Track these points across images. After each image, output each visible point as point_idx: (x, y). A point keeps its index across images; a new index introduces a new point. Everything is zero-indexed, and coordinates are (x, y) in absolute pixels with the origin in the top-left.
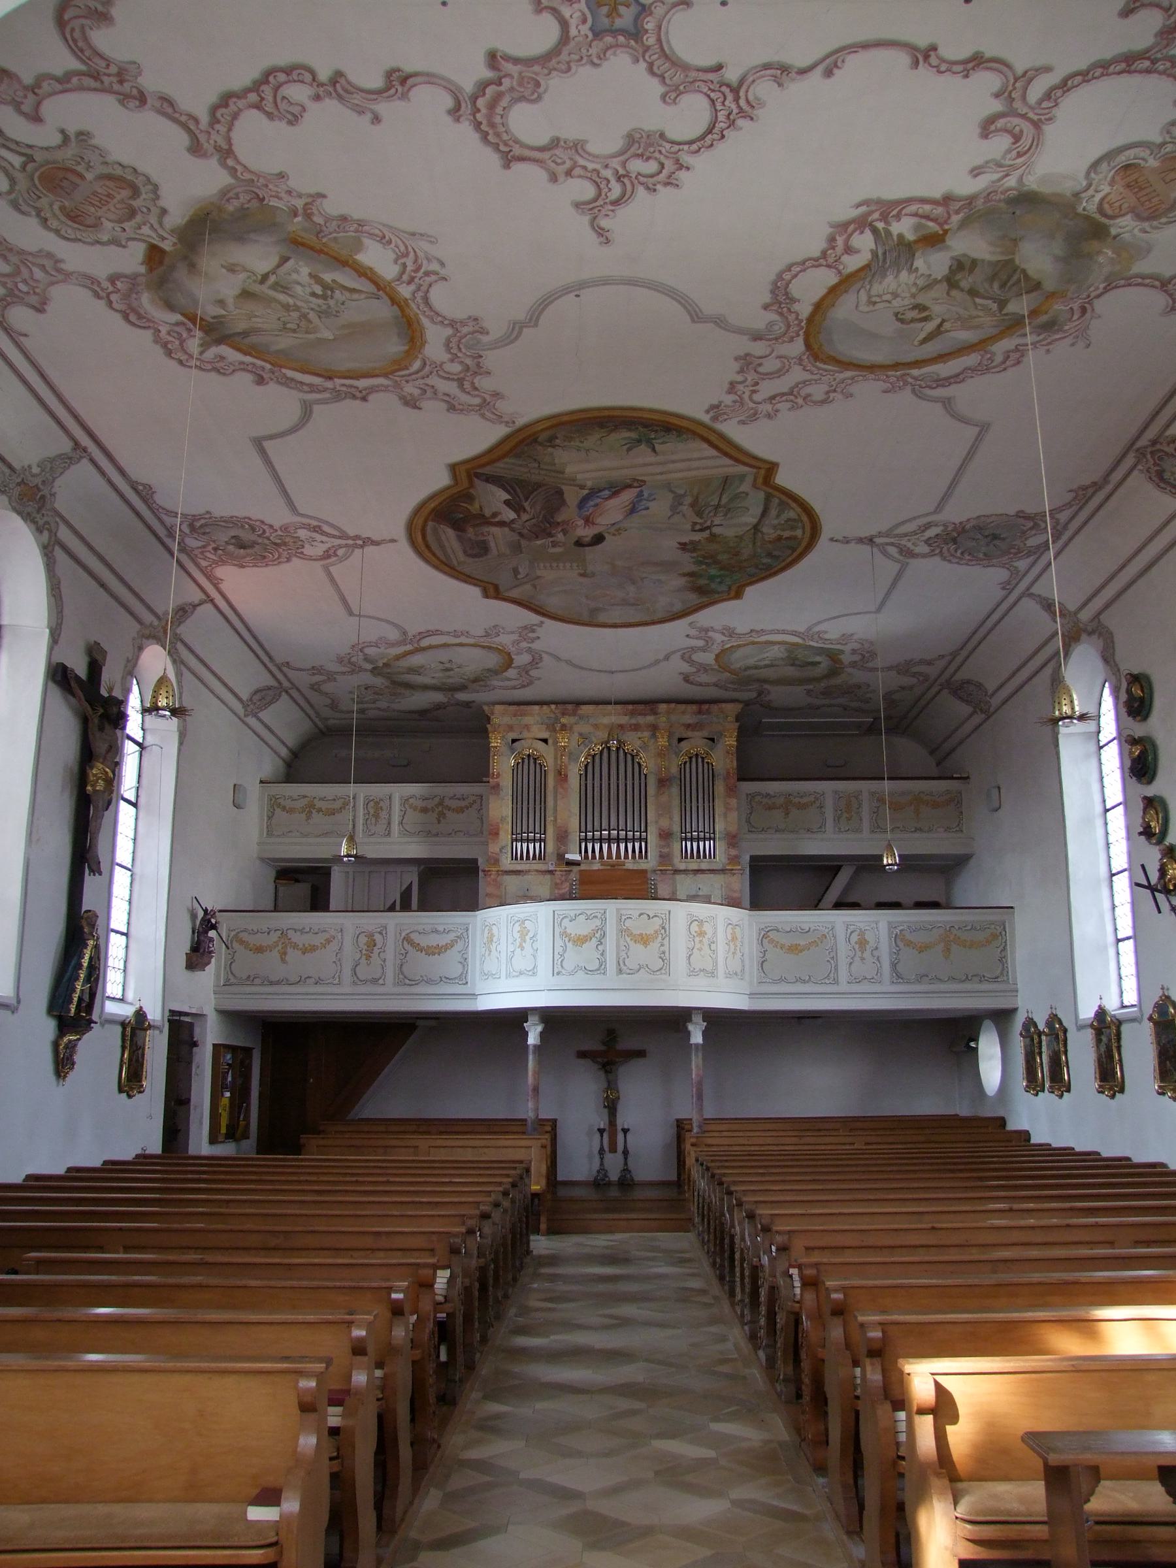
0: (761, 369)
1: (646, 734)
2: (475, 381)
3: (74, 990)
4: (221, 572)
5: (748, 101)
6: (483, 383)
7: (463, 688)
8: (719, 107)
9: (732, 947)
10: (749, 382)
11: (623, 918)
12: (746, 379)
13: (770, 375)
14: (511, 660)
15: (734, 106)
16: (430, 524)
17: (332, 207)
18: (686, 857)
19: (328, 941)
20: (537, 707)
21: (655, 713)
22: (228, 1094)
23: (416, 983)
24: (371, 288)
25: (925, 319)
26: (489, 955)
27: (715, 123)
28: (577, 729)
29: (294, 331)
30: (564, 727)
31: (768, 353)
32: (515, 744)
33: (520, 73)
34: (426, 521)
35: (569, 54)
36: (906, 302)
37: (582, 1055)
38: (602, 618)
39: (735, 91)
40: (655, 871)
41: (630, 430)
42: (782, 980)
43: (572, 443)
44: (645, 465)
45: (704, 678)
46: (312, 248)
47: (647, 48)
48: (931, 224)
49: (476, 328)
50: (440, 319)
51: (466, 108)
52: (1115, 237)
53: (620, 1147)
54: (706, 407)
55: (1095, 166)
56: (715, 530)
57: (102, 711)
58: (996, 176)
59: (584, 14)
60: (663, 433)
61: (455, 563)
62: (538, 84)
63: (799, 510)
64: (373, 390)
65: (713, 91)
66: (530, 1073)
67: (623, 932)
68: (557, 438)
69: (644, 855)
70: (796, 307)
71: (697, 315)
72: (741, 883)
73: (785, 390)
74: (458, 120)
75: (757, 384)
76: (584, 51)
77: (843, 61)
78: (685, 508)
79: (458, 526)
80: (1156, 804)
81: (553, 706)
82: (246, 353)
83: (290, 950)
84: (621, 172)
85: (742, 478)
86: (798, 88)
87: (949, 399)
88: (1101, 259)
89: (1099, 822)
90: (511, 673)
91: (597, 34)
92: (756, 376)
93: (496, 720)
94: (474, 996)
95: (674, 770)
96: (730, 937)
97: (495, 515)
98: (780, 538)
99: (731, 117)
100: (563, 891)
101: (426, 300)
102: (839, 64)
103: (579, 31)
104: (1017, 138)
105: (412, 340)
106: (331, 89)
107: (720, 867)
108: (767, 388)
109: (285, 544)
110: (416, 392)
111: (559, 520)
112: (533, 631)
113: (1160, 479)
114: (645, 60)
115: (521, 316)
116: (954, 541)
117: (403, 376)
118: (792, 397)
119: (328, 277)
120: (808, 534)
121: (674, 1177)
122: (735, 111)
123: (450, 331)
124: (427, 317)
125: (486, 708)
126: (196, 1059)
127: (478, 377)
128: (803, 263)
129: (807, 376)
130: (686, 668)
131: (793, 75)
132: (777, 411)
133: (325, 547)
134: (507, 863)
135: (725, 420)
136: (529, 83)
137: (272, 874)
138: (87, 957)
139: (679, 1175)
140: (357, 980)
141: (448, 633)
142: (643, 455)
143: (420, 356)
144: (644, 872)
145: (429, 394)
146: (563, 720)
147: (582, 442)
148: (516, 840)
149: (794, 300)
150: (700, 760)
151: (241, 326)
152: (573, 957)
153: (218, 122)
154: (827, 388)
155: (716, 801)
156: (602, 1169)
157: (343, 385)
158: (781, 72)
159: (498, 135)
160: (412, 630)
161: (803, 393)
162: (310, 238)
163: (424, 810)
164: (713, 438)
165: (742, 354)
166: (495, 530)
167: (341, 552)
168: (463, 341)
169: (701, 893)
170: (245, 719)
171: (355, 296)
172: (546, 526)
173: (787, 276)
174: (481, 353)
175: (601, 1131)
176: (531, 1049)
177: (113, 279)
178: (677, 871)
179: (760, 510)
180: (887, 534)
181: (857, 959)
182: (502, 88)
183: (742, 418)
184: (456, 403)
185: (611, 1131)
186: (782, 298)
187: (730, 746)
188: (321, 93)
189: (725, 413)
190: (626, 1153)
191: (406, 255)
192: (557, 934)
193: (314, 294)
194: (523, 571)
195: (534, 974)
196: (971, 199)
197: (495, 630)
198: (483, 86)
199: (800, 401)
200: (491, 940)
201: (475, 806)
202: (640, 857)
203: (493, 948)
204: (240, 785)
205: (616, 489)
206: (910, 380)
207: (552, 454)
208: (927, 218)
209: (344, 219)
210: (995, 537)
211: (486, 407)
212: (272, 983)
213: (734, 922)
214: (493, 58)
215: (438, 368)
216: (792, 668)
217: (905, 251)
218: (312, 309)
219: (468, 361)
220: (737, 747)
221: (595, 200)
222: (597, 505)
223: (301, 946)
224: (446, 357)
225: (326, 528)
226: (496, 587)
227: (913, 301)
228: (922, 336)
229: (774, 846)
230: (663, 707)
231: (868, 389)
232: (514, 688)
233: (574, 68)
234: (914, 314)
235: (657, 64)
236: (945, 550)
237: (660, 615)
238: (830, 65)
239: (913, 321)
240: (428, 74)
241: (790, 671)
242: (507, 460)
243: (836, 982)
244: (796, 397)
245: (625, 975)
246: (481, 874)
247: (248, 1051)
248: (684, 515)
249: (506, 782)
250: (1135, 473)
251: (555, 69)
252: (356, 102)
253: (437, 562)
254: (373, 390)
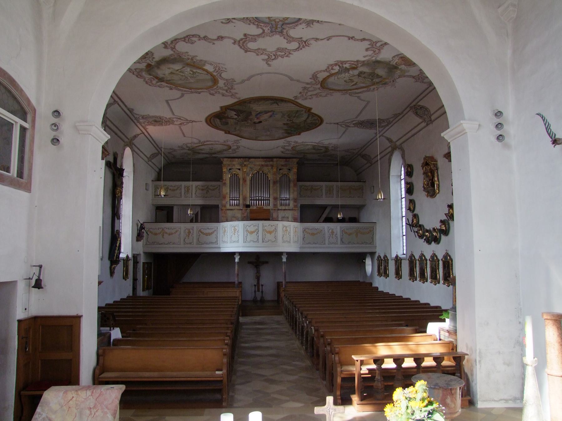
1: (270, 168)
3: (115, 253)
4: (147, 127)
5: (308, 43)
6: (233, 91)
7: (215, 153)
9: (295, 234)
11: (264, 226)
13: (310, 91)
14: (231, 148)
17: (198, 58)
18: (281, 205)
19: (176, 232)
20: (237, 159)
21: (272, 161)
22: (146, 277)
23: (202, 244)
24: (207, 73)
25: (352, 82)
26: (225, 236)
28: (249, 166)
29: (183, 80)
30: (245, 165)
32: (231, 170)
34: (211, 118)
36: (348, 79)
37: (249, 263)
38: (259, 139)
40: (272, 209)
41: (271, 101)
42: (309, 243)
45: (288, 152)
46: (192, 66)
48: (353, 65)
52: (400, 69)
53: (261, 290)
55: (394, 57)
56: (293, 121)
57: (119, 173)
58: (369, 58)
61: (218, 126)
63: (317, 117)
66: (236, 270)
67: (264, 230)
69: (269, 205)
70: (318, 79)
72: (297, 214)
78: (286, 116)
79: (220, 119)
80: (412, 202)
81: (242, 159)
82: (168, 84)
83: (165, 234)
84: (275, 54)
85: (302, 111)
86: (320, 42)
87: (359, 96)
88: (397, 72)
89: (400, 201)
90: (230, 150)
91: (271, 32)
92: (307, 91)
93: (224, 163)
94: (220, 248)
95: (278, 179)
96: (294, 231)
97: (231, 117)
98: (312, 123)
100: (245, 215)
101: (220, 75)
104: (374, 52)
107: (291, 208)
108: (309, 93)
109: (169, 121)
111: (250, 118)
112: (238, 141)
113: (416, 114)
116: (361, 124)
118: (317, 95)
119: (195, 71)
120: (320, 121)
121: (276, 299)
123: (225, 81)
125: (221, 159)
126: (138, 267)
128: (321, 71)
129: (320, 91)
130: (282, 150)
132: (313, 98)
133: (180, 122)
134: (228, 207)
137: (155, 208)
138: (118, 243)
139: (278, 299)
140: (185, 243)
141: (213, 141)
142: (275, 106)
144: (269, 209)
145: (218, 92)
146: (245, 163)
148: (231, 200)
149: (317, 78)
150: (286, 175)
151: (169, 79)
152: (249, 237)
153: (173, 43)
154: (326, 94)
155: (291, 188)
156: (255, 297)
158: (317, 39)
159: (244, 47)
160: (202, 140)
161: (320, 94)
162: (192, 64)
163: (202, 190)
164: (294, 103)
166: (232, 120)
167: (185, 123)
169: (285, 216)
170: (148, 163)
171: (201, 74)
172: (246, 119)
173: (316, 73)
175: (255, 285)
176: (236, 263)
177: (136, 69)
178: (278, 210)
179: (306, 117)
180: (342, 122)
181: (331, 238)
183: (303, 99)
185: (258, 285)
187: (295, 172)
190: (262, 292)
191: (217, 67)
192: (245, 231)
193: (190, 74)
194: (237, 128)
195: (238, 242)
196: (364, 61)
197: (227, 141)
198: (242, 39)
199: (319, 96)
200: (225, 231)
201: (218, 188)
202: (268, 205)
203: (226, 234)
204: (148, 184)
205: (266, 112)
208: (353, 64)
209: (201, 60)
210: (372, 123)
211: (233, 96)
212: (160, 244)
213: (296, 226)
214: (245, 35)
215: (221, 88)
216: (314, 150)
217: (347, 70)
218: (189, 76)
219: (230, 87)
220: (297, 172)
221: (268, 59)
222: (261, 115)
223: (168, 233)
224: (224, 86)
225: (182, 118)
228: (351, 85)
229: (307, 201)
230: (275, 160)
231: (338, 94)
232: (231, 154)
236: (358, 125)
237: (276, 138)
238: (329, 39)
239: (349, 82)
241: (314, 151)
243: (325, 244)
245: (265, 243)
246: (220, 209)
247: (151, 263)
249: (228, 182)
250: (410, 112)
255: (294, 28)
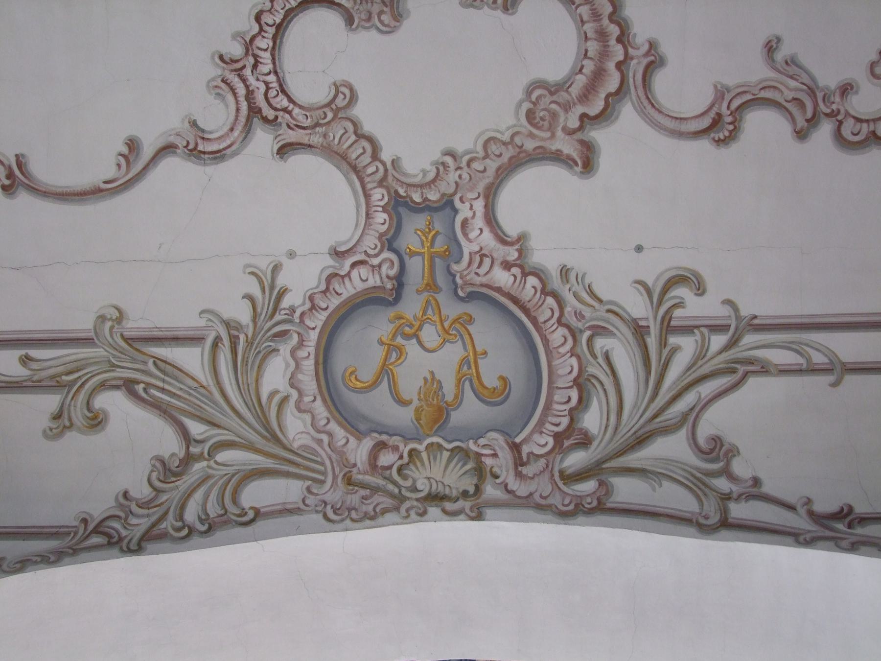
8: (272, 78)
15: (252, 80)
27: (274, 48)
33: (553, 136)
35: (485, 170)
39: (254, 111)
47: (381, 183)
51: (636, 68)
59: (465, 235)
62: (530, 116)
65: (285, 110)
74: (652, 45)
76: (465, 176)
77: (119, 165)
91: (447, 204)
99: (251, 60)
102: (123, 161)
103: (471, 208)
106: (822, 107)
114: (384, 164)
122: (248, 72)
131: (181, 143)
136: (542, 119)
182: (580, 109)
188: (837, 99)
198: (605, 116)
233: (479, 148)
235: (366, 159)
240: (680, 135)
251: (505, 144)
252: (793, 84)
255: (337, 254)
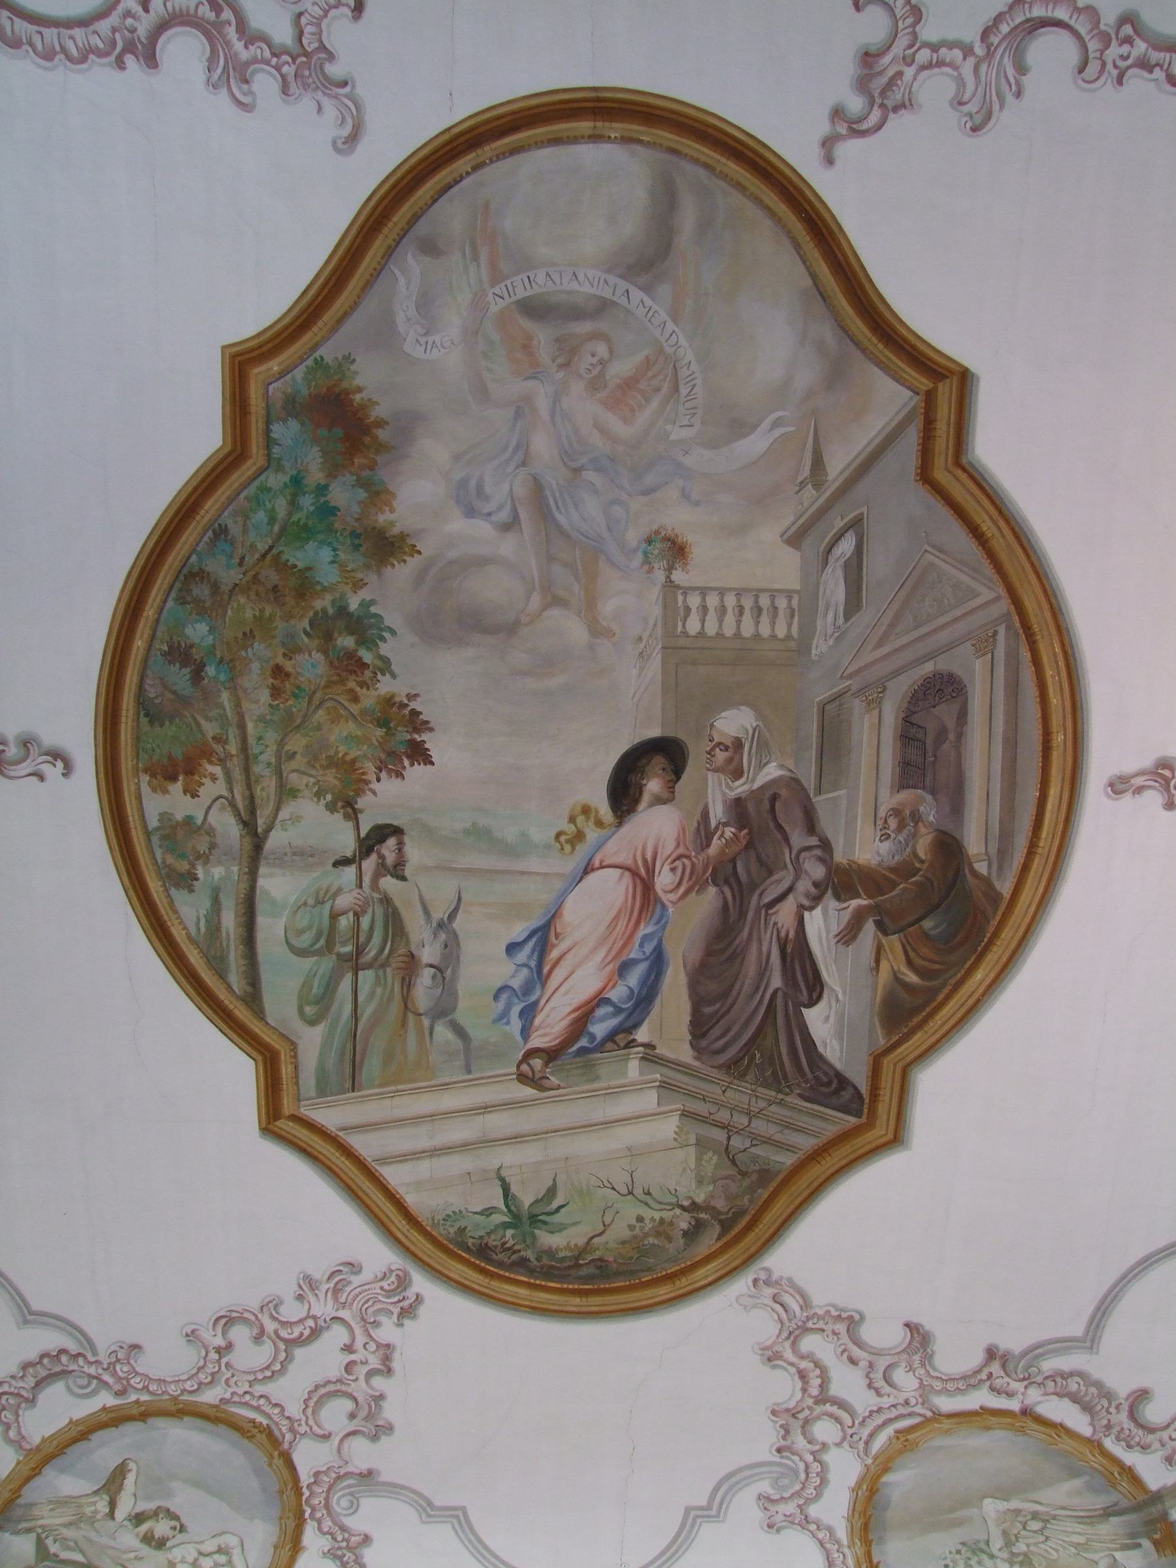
0: (349, 1405)
2: (799, 1395)
10: (362, 1371)
12: (367, 1381)
16: (1005, 888)
25: (138, 1519)
31: (346, 1444)
36: (176, 1554)
41: (550, 1253)
43: (657, 1216)
44: (517, 1139)
49: (773, 1508)
50: (820, 1535)
54: (422, 1311)
60: (493, 1241)
64: (969, 1381)
68: (686, 1234)
70: (325, 1543)
71: (460, 1522)
73: (299, 1353)
75: (349, 1367)
87: (26, 1322)
92: (352, 1388)
105: (873, 1491)
110: (899, 1375)
115: (708, 1532)
117: (910, 1415)
118: (284, 1334)
123: (813, 1511)
124: (838, 1542)
127: (792, 1404)
135: (384, 1277)
143: (869, 1461)
147: (640, 1219)
149: (332, 1554)
157: (1010, 1395)
165: (384, 1438)
168: (798, 1487)
174: (776, 1458)
183: (356, 1280)
184: (845, 1338)
186: (349, 1556)
189: (389, 1293)
194: (835, 588)
199: (270, 1327)
206: (107, 1377)
207: (700, 1182)
219: (800, 1442)
222: (624, 968)
224: (831, 1457)
226: (925, 476)
227: (170, 1557)
234: (162, 1528)
239: (155, 1514)
242: (788, 1160)
244: (276, 1332)
248: (427, 912)
253: (1048, 649)
254: (969, 1381)
